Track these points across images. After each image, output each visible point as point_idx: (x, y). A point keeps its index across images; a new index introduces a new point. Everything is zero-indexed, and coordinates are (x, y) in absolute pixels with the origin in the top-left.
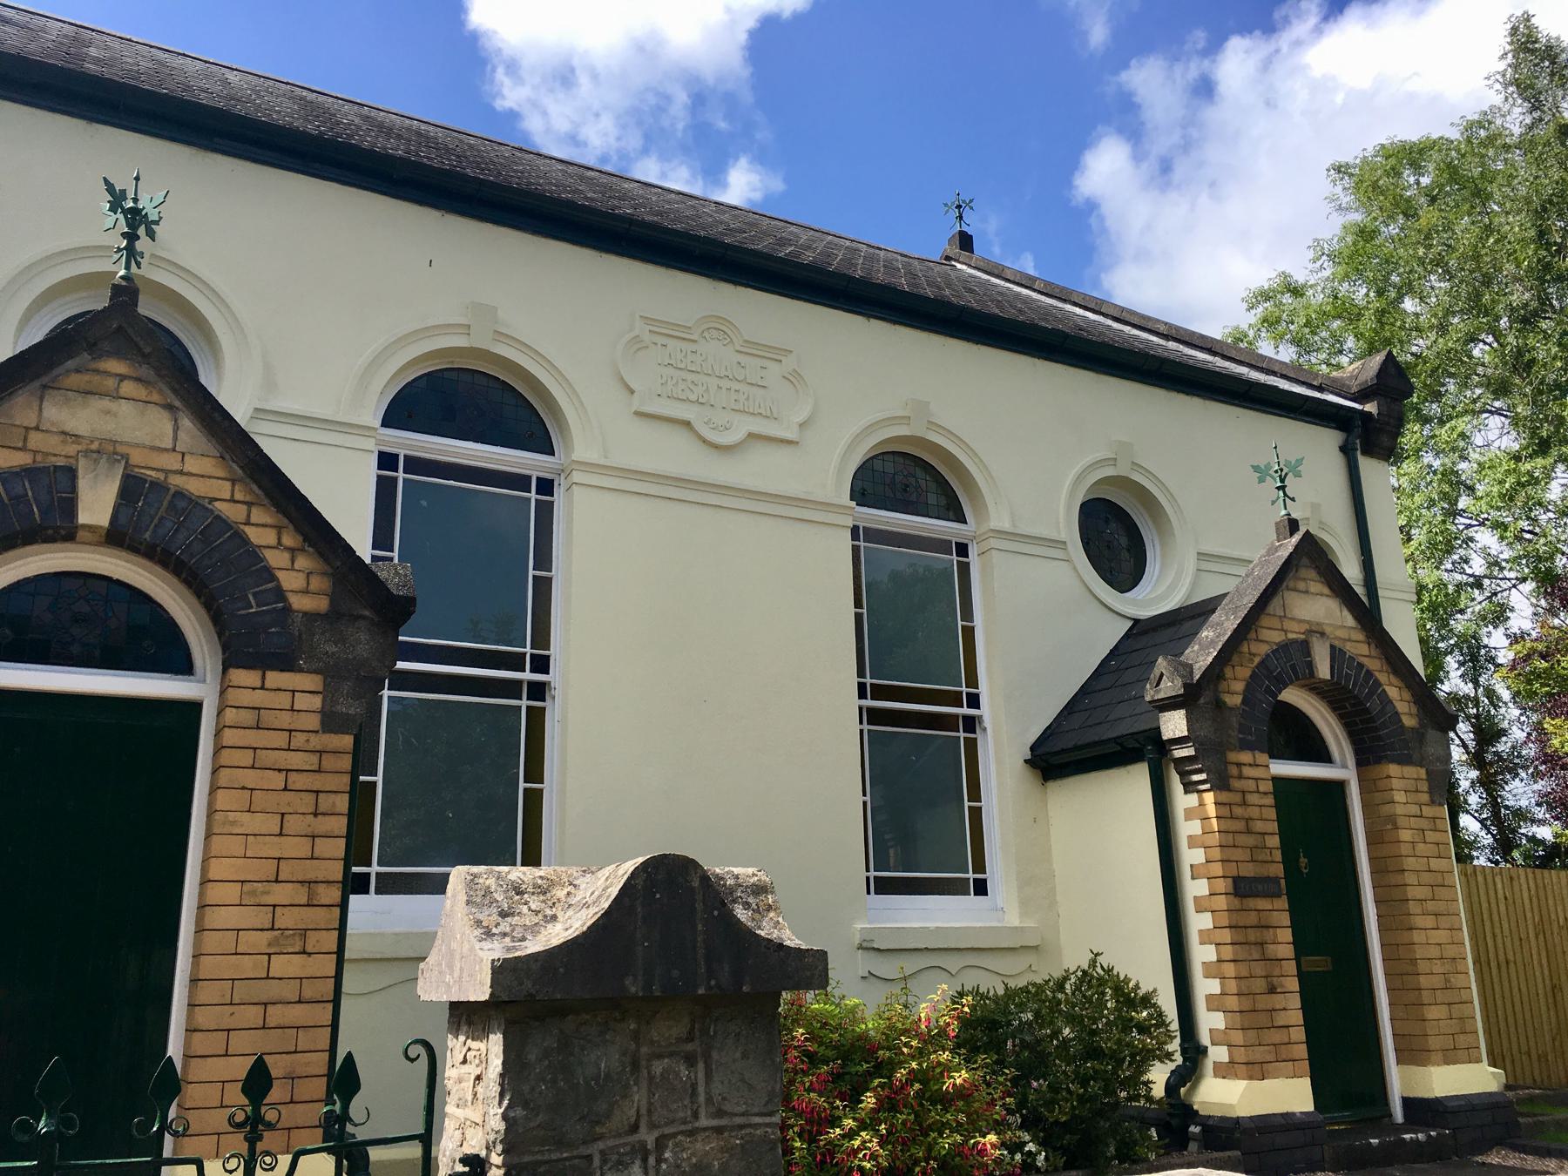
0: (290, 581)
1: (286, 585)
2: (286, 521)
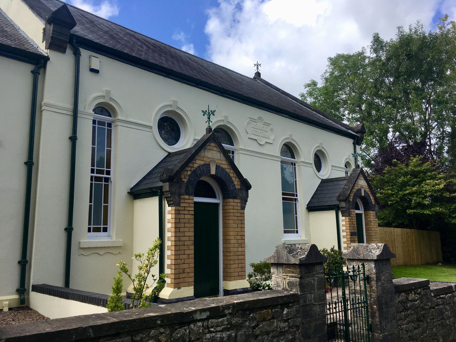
0: (236, 183)
1: (235, 184)
2: (234, 172)
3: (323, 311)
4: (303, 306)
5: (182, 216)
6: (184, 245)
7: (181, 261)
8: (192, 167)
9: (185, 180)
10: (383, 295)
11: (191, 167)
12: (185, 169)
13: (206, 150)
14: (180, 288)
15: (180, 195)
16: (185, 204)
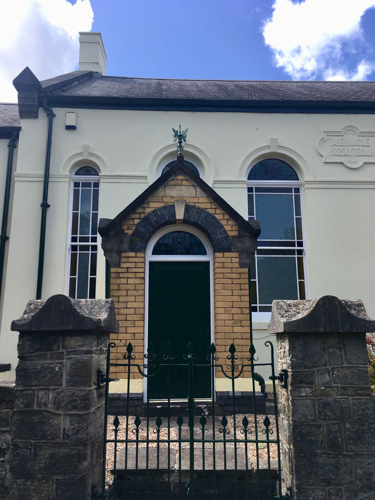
0: (227, 228)
1: (227, 230)
2: (225, 212)
3: (79, 430)
4: (20, 413)
5: (124, 281)
6: (126, 320)
7: (121, 341)
8: (142, 213)
9: (130, 232)
10: (320, 422)
11: (140, 213)
12: (130, 217)
13: (167, 188)
14: (119, 380)
15: (119, 252)
16: (128, 264)
